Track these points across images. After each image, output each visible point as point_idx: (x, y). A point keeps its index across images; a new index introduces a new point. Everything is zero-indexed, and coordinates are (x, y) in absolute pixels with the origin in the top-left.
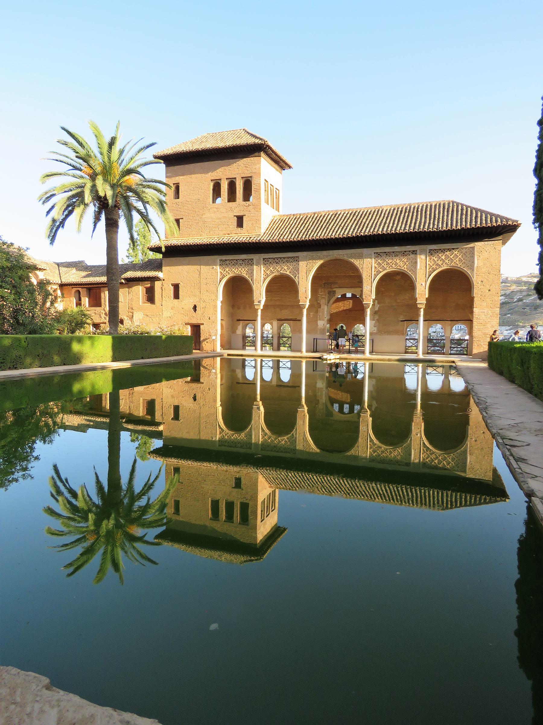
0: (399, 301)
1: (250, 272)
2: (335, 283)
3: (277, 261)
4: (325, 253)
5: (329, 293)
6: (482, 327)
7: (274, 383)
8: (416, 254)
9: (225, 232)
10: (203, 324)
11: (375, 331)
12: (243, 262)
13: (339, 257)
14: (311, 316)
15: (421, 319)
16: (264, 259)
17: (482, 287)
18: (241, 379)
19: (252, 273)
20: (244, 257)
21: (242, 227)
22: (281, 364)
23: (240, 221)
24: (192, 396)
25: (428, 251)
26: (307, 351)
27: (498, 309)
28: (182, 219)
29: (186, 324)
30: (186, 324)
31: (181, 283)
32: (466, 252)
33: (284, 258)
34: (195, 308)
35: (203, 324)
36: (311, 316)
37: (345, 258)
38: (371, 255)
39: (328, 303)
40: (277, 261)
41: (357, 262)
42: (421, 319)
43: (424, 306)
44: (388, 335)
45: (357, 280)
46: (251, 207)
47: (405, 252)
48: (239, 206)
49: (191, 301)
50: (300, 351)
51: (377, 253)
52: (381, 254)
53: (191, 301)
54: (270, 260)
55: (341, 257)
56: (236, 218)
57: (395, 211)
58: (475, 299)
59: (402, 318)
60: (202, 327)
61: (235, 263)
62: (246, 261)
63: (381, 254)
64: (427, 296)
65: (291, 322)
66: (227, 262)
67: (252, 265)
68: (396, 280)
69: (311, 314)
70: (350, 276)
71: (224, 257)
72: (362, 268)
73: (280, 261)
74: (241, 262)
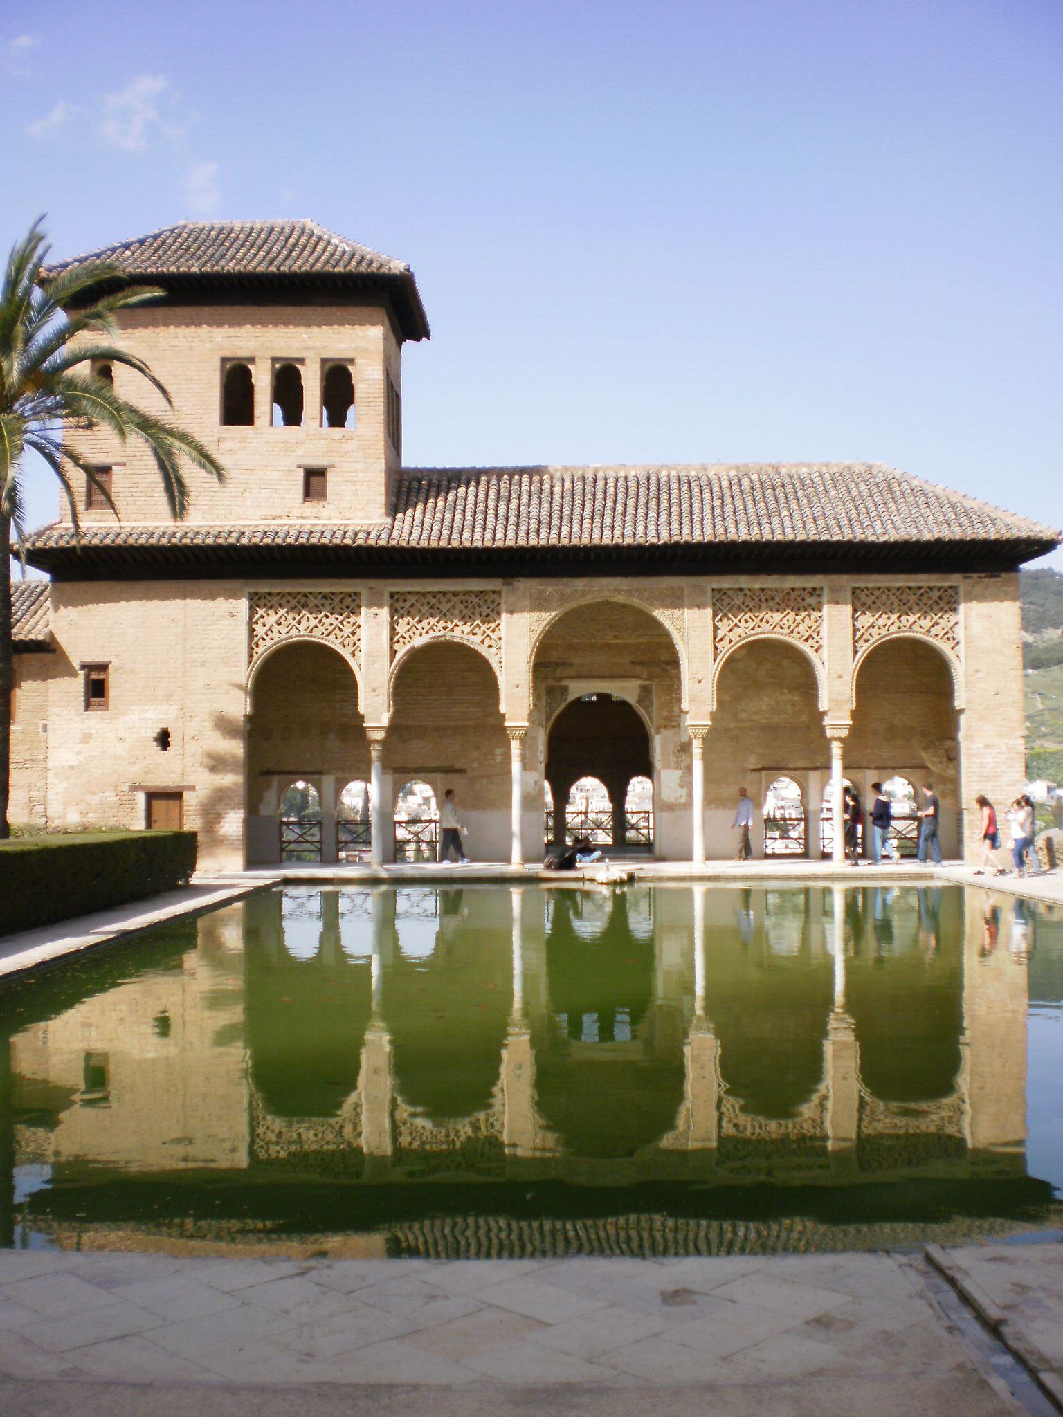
0: (743, 716)
1: (348, 630)
2: (565, 664)
5: (551, 691)
8: (819, 596)
10: (192, 788)
11: (683, 800)
12: (327, 602)
14: (499, 759)
15: (837, 765)
16: (392, 595)
19: (353, 633)
20: (325, 586)
22: (402, 904)
23: (314, 481)
24: (154, 1011)
25: (849, 593)
26: (526, 859)
27: (1022, 741)
28: (124, 464)
29: (134, 788)
30: (134, 788)
31: (115, 662)
32: (940, 598)
33: (455, 594)
34: (163, 739)
35: (192, 788)
36: (499, 759)
38: (703, 593)
39: (548, 719)
40: (433, 601)
41: (663, 615)
42: (837, 765)
43: (844, 733)
44: (717, 808)
45: (661, 661)
47: (793, 589)
48: (313, 437)
49: (149, 715)
50: (508, 860)
51: (719, 590)
52: (730, 593)
53: (149, 715)
54: (412, 599)
56: (301, 473)
57: (745, 482)
59: (753, 762)
60: (186, 795)
61: (299, 604)
65: (439, 776)
67: (355, 611)
69: (498, 751)
70: (608, 646)
71: (264, 587)
73: (444, 600)
74: (318, 602)
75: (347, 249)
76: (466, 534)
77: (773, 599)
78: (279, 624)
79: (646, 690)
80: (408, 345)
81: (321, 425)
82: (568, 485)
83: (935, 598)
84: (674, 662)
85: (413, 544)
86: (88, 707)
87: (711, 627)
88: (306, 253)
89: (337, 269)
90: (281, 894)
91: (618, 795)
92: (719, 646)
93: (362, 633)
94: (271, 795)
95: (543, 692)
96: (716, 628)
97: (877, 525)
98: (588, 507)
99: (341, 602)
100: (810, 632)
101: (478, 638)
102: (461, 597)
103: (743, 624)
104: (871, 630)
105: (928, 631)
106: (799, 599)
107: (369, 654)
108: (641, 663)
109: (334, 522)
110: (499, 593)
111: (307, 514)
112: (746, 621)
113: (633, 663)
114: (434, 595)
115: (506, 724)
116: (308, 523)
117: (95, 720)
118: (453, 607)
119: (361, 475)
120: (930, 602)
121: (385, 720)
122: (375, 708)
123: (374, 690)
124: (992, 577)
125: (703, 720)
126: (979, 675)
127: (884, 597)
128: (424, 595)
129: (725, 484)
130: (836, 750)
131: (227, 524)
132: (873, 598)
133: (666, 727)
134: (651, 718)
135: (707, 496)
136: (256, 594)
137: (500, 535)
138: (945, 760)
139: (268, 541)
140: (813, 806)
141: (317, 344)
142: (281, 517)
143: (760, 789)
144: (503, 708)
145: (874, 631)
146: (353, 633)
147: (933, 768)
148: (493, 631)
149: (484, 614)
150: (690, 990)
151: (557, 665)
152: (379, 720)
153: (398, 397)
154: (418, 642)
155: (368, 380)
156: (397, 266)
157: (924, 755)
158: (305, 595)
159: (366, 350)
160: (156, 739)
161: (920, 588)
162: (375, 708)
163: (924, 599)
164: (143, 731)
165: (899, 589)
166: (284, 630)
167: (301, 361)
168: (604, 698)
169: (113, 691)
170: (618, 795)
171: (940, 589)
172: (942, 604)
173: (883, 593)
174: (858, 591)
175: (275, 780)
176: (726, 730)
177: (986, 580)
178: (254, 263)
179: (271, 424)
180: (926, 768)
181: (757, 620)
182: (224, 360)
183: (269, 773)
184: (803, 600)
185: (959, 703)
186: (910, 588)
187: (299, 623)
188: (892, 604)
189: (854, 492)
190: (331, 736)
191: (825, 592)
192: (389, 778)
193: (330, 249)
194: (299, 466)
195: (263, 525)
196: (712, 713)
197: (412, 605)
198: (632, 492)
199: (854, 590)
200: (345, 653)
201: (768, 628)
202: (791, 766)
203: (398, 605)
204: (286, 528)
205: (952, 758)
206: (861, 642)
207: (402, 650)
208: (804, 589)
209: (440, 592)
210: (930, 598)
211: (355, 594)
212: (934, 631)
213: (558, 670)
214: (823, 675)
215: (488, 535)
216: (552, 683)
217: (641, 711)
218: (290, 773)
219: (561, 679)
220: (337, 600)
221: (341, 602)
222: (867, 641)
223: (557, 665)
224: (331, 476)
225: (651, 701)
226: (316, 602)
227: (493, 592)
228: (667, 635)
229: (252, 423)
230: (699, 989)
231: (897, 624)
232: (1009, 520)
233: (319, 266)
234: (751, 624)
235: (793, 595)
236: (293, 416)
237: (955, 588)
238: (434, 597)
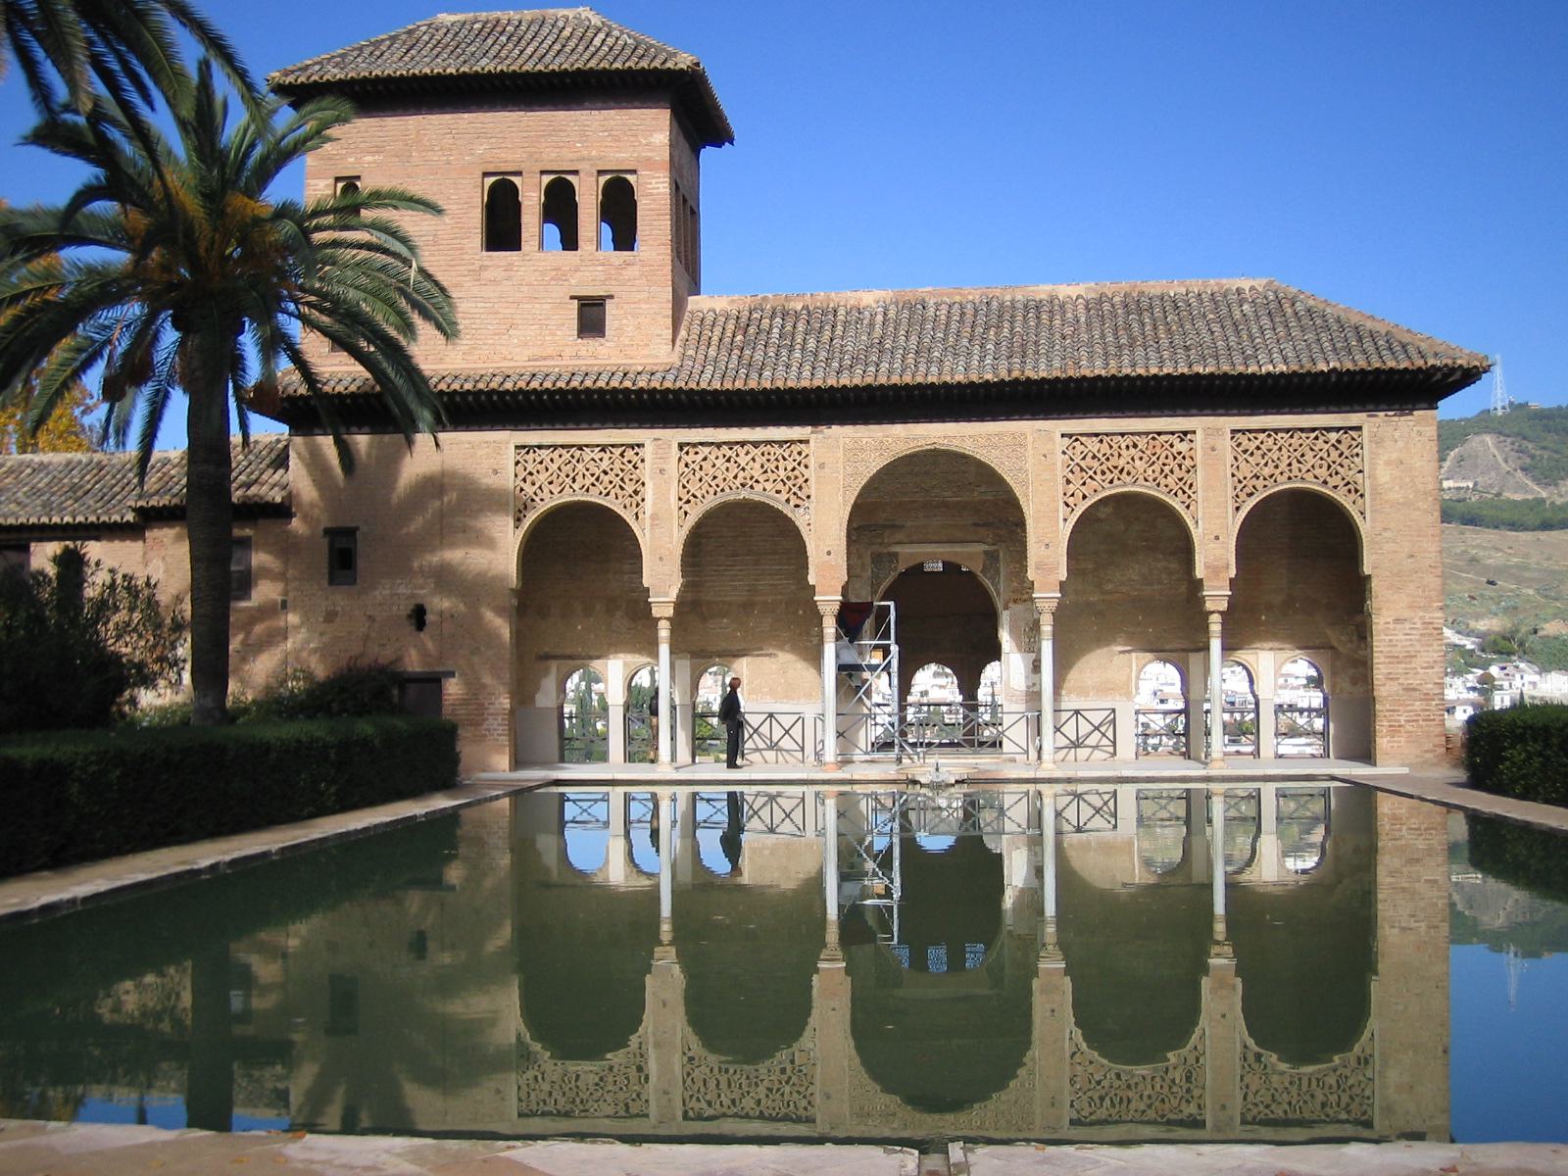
0: (1110, 587)
1: (630, 488)
3: (729, 453)
4: (899, 430)
5: (877, 559)
6: (1400, 668)
7: (686, 877)
8: (1191, 441)
9: (537, 351)
12: (606, 456)
13: (944, 444)
15: (1216, 645)
16: (681, 446)
17: (1390, 546)
18: (555, 873)
21: (603, 336)
23: (591, 316)
31: (364, 529)
32: (1339, 441)
33: (756, 444)
37: (968, 448)
38: (1052, 439)
40: (729, 453)
42: (1216, 645)
43: (1223, 606)
46: (633, 272)
47: (1159, 434)
51: (1070, 436)
53: (402, 590)
54: (706, 450)
55: (956, 446)
57: (1106, 307)
58: (1374, 583)
62: (617, 452)
63: (1083, 439)
64: (1233, 573)
66: (544, 453)
68: (1099, 520)
70: (945, 504)
72: (1025, 484)
73: (742, 451)
75: (629, 41)
76: (767, 373)
77: (1135, 446)
78: (551, 483)
79: (992, 557)
80: (708, 154)
81: (599, 246)
82: (892, 314)
83: (1333, 441)
84: (1021, 523)
85: (703, 385)
86: (332, 582)
87: (1061, 481)
88: (581, 48)
89: (614, 66)
90: (563, 799)
91: (969, 685)
92: (1071, 501)
93: (649, 492)
94: (549, 683)
95: (868, 560)
96: (1068, 482)
97: (1262, 357)
98: (914, 339)
99: (622, 455)
100: (1181, 484)
101: (784, 496)
102: (762, 448)
103: (1098, 477)
104: (1254, 481)
105: (1325, 482)
106: (1167, 446)
107: (654, 517)
108: (984, 525)
109: (613, 361)
110: (807, 442)
111: (583, 353)
112: (1103, 473)
113: (976, 525)
114: (731, 444)
115: (815, 598)
116: (583, 364)
117: (340, 599)
118: (753, 459)
119: (644, 306)
120: (1326, 447)
121: (673, 594)
122: (662, 578)
123: (661, 559)
124: (1401, 416)
125: (1054, 591)
126: (1387, 534)
127: (1271, 441)
128: (719, 445)
129: (1081, 308)
130: (1215, 625)
131: (489, 367)
132: (1258, 442)
133: (1015, 602)
134: (998, 594)
135: (1057, 322)
136: (524, 447)
137: (806, 374)
138: (1355, 638)
139: (535, 384)
140: (1192, 696)
141: (594, 153)
142: (551, 357)
143: (1130, 677)
144: (811, 580)
145: (1260, 483)
146: (636, 492)
147: (1341, 649)
148: (800, 488)
149: (789, 468)
150: (1041, 912)
151: (885, 527)
152: (666, 595)
153: (694, 213)
154: (711, 502)
155: (653, 194)
156: (683, 61)
157: (1328, 632)
158: (580, 448)
159: (648, 159)
160: (409, 617)
161: (1313, 430)
162: (662, 578)
163: (1320, 443)
164: (395, 608)
165: (1287, 431)
166: (556, 489)
167: (575, 172)
168: (951, 567)
169: (361, 563)
170: (969, 685)
171: (1338, 429)
172: (1342, 447)
173: (1269, 436)
174: (1237, 436)
175: (554, 665)
176: (1088, 604)
177: (1396, 419)
178: (520, 61)
179: (541, 245)
180: (1332, 648)
181: (1116, 472)
182: (486, 174)
183: (547, 657)
184: (1172, 446)
185: (1367, 570)
186: (1302, 430)
187: (574, 480)
188: (1280, 449)
189: (1237, 315)
190: (619, 614)
191: (1199, 437)
192: (685, 665)
193: (610, 41)
194: (572, 298)
195: (531, 367)
196: (1061, 583)
197: (705, 459)
198: (969, 318)
199: (1234, 432)
200: (628, 516)
201: (1128, 479)
202: (1167, 647)
203: (688, 459)
204: (557, 370)
205: (1362, 632)
206: (1242, 496)
207: (696, 513)
208: (1173, 433)
209: (737, 443)
210: (1326, 442)
211: (638, 446)
212: (1332, 482)
213: (886, 535)
214: (1197, 534)
215: (793, 373)
216: (877, 548)
217: (987, 583)
218: (571, 657)
219: (890, 545)
220: (617, 452)
221: (622, 455)
222: (1250, 495)
223: (885, 527)
224: (610, 307)
225: (997, 572)
226: (592, 455)
227: (801, 442)
228: (1009, 491)
229: (520, 249)
230: (1050, 909)
231: (1286, 475)
232: (1423, 346)
233: (592, 64)
234: (1109, 477)
235: (1163, 438)
236: (570, 242)
237: (1359, 428)
238: (731, 449)
